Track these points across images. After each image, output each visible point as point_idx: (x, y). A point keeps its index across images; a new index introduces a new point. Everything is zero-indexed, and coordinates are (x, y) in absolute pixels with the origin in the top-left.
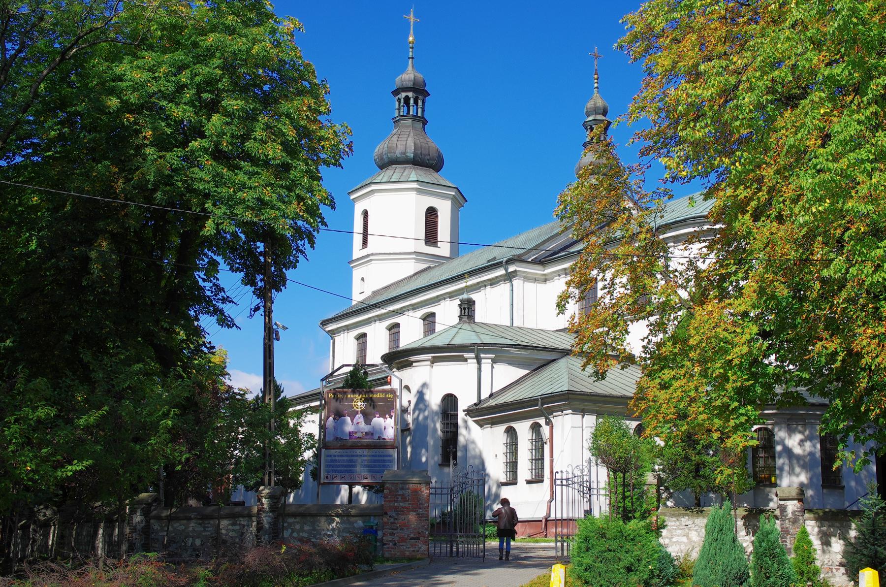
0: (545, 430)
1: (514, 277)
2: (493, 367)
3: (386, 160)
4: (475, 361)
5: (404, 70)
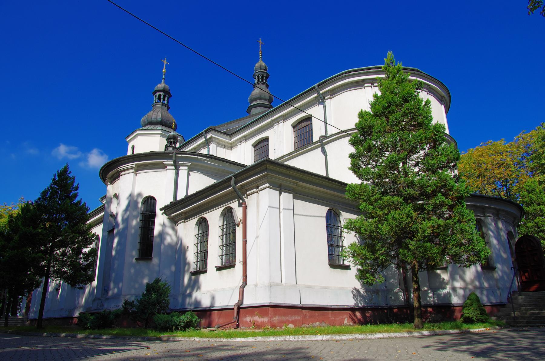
0: (238, 212)
1: (210, 142)
2: (189, 175)
3: (147, 122)
4: (173, 167)
5: (160, 82)
